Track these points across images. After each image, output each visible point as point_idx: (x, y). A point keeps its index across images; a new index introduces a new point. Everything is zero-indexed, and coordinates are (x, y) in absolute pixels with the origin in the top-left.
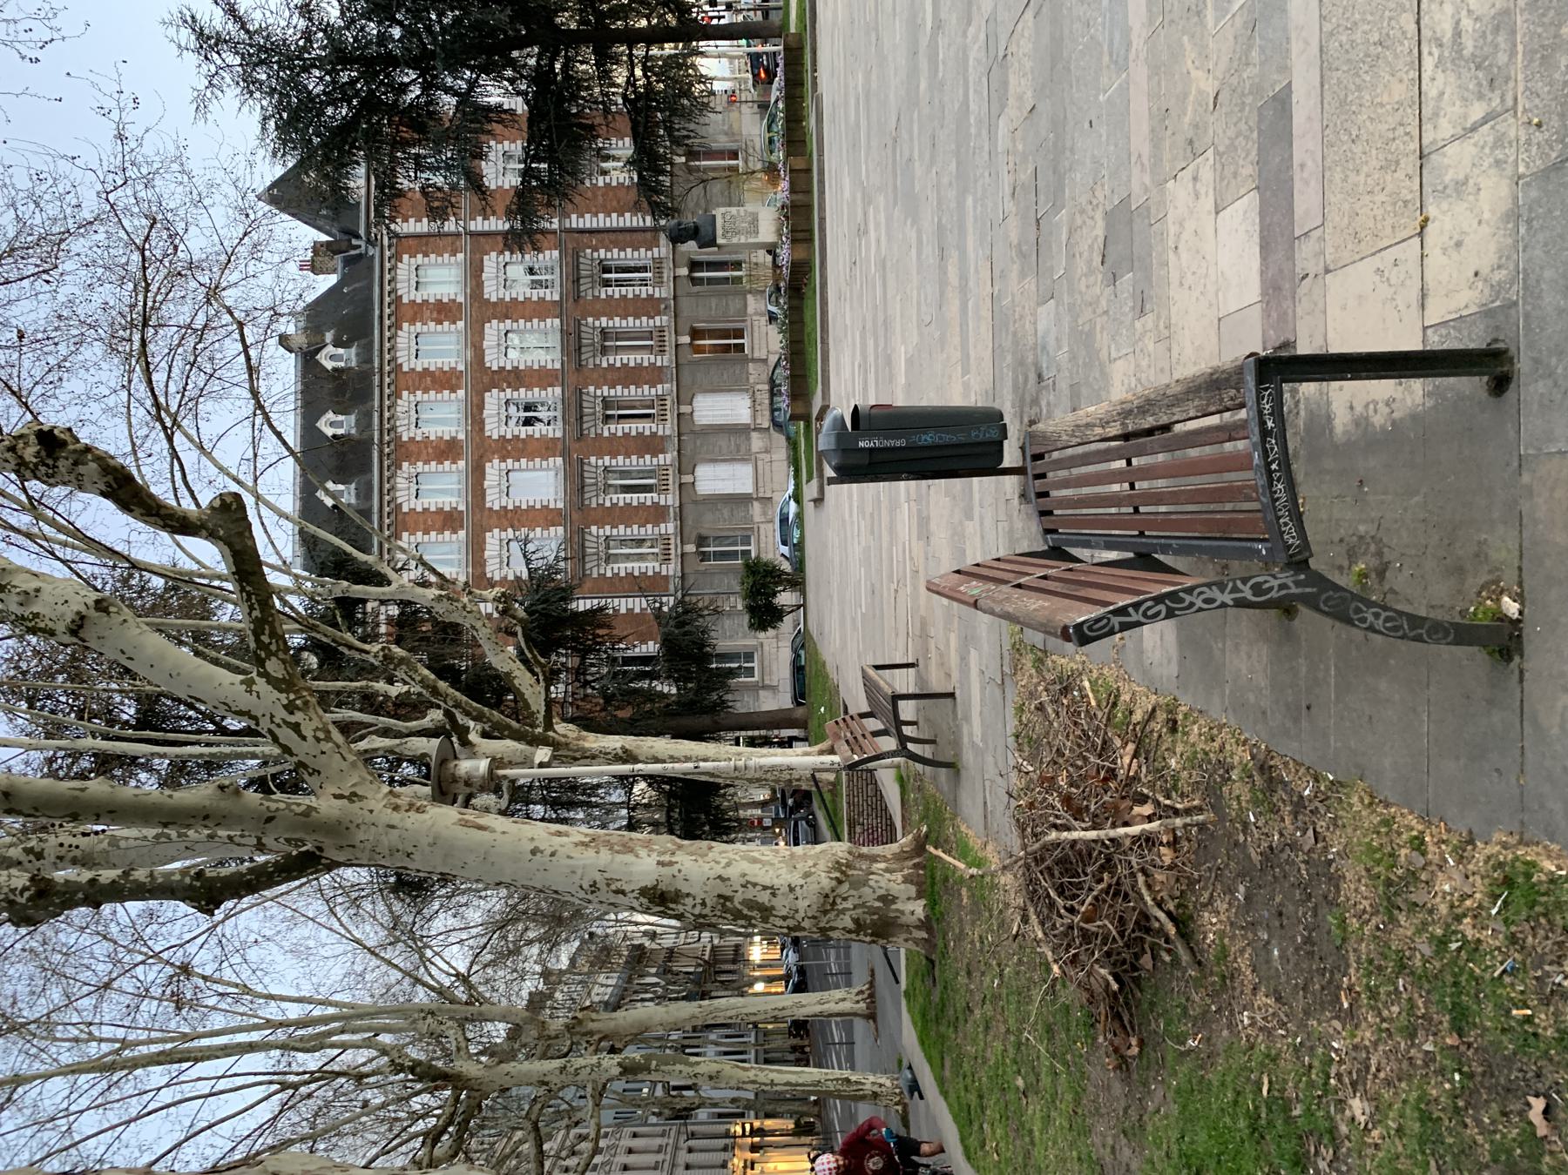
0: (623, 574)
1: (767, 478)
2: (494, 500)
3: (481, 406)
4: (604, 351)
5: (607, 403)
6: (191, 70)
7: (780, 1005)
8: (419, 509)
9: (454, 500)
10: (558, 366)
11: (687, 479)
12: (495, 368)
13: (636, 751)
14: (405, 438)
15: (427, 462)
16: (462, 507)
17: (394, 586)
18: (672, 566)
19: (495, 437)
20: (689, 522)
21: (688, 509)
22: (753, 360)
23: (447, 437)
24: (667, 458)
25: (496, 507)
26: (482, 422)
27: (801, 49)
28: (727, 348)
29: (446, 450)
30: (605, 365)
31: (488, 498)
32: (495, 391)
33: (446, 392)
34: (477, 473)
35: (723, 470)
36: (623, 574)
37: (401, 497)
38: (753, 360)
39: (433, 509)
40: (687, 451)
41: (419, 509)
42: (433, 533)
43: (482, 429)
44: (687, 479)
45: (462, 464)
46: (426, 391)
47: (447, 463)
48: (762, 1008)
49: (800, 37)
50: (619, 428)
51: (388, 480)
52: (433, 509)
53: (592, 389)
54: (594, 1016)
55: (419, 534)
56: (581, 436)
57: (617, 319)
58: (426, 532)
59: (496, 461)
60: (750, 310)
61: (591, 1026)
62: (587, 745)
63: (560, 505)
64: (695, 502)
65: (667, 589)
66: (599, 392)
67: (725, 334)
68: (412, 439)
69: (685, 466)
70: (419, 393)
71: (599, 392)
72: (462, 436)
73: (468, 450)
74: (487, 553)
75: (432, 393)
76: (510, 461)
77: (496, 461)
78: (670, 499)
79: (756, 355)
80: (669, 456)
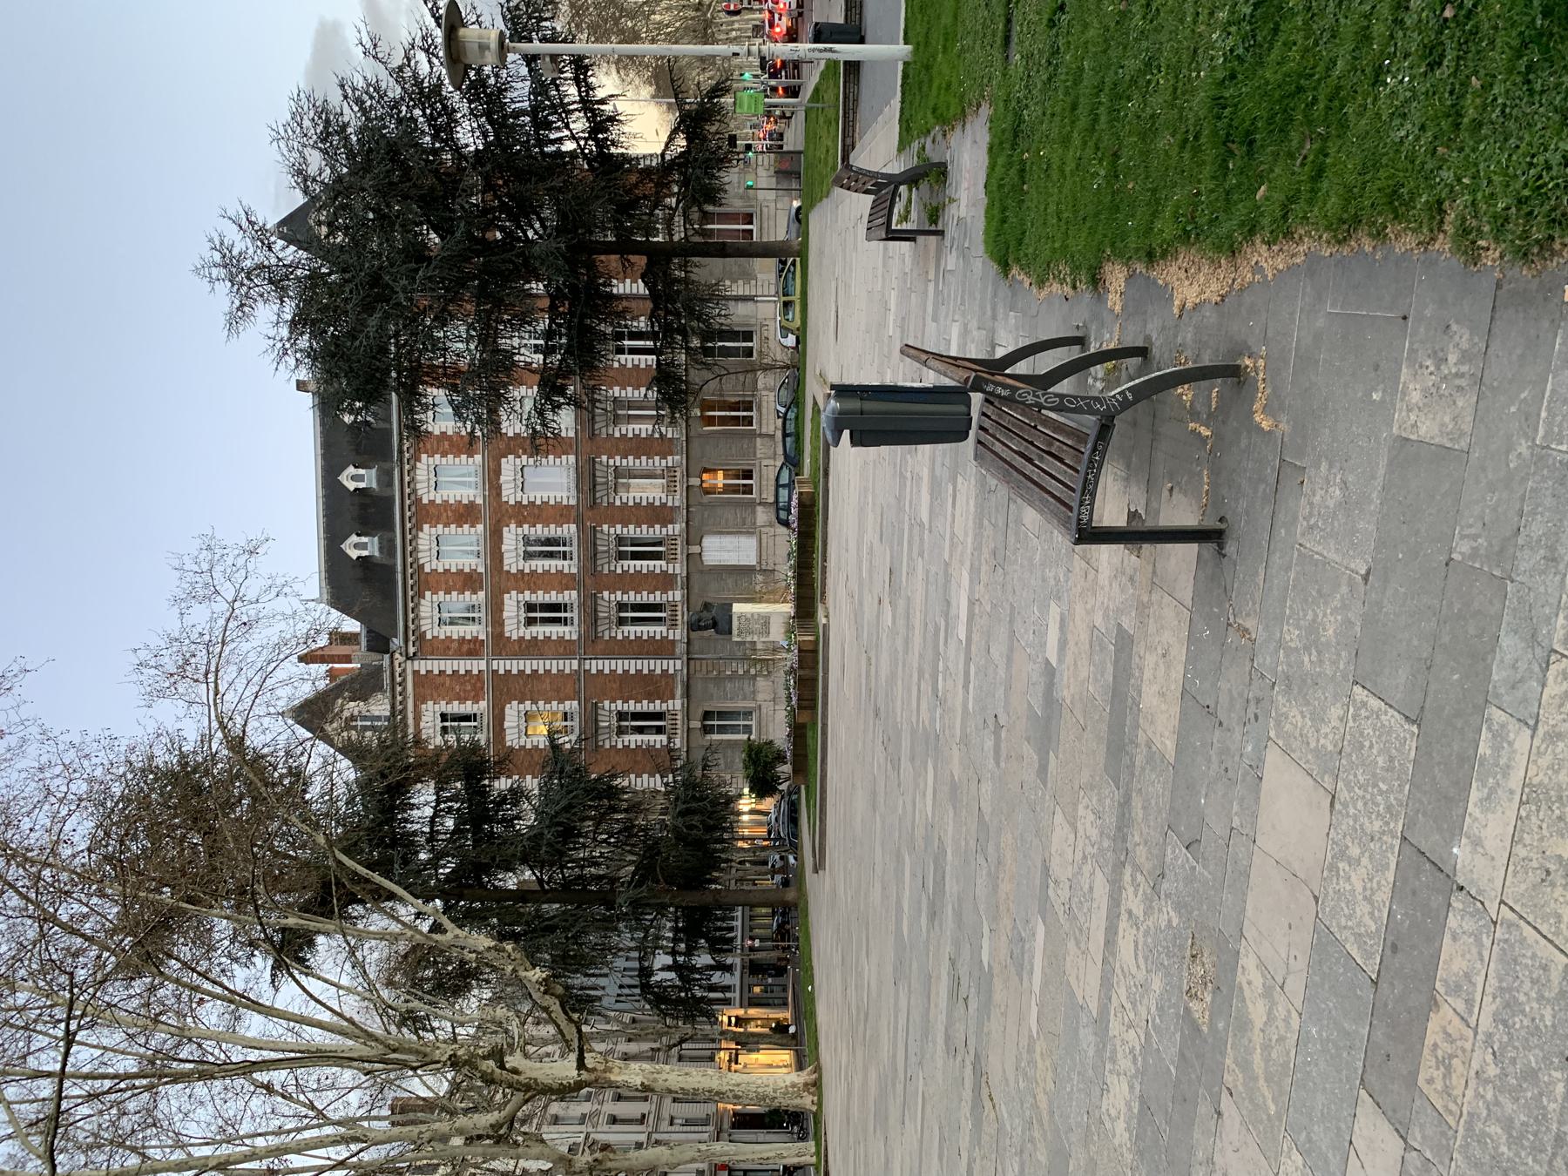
0: (632, 637)
1: (771, 551)
3: (498, 472)
4: (617, 420)
5: (621, 540)
6: (223, 297)
7: (765, 1155)
8: (441, 570)
9: (472, 492)
11: (695, 549)
12: (511, 434)
13: (654, 1085)
14: (425, 501)
15: (446, 525)
16: (481, 570)
17: (449, 936)
18: (678, 631)
19: (512, 502)
20: (695, 590)
21: (695, 578)
22: (761, 435)
23: (465, 501)
24: (676, 528)
25: (514, 571)
26: (499, 487)
27: (813, 504)
28: (736, 420)
29: (464, 514)
30: (617, 435)
31: (506, 562)
32: (511, 457)
33: (464, 457)
34: (495, 538)
35: (728, 541)
36: (632, 637)
37: (424, 557)
38: (761, 435)
39: (454, 570)
40: (694, 523)
41: (441, 570)
42: (454, 593)
43: (499, 495)
44: (695, 549)
45: (480, 527)
46: (444, 455)
47: (466, 526)
48: (750, 1157)
49: (813, 497)
51: (410, 543)
52: (454, 570)
53: (604, 458)
54: (611, 1156)
55: (441, 593)
56: (594, 504)
57: (630, 389)
58: (448, 592)
59: (513, 526)
60: (760, 385)
61: (609, 1165)
62: (613, 1078)
64: (702, 572)
65: (673, 652)
66: (611, 462)
67: (735, 407)
68: (432, 502)
69: (693, 537)
70: (437, 456)
71: (611, 462)
72: (479, 501)
73: (486, 513)
74: (505, 614)
75: (450, 457)
76: (526, 526)
77: (513, 526)
78: (678, 568)
79: (764, 431)
80: (677, 527)
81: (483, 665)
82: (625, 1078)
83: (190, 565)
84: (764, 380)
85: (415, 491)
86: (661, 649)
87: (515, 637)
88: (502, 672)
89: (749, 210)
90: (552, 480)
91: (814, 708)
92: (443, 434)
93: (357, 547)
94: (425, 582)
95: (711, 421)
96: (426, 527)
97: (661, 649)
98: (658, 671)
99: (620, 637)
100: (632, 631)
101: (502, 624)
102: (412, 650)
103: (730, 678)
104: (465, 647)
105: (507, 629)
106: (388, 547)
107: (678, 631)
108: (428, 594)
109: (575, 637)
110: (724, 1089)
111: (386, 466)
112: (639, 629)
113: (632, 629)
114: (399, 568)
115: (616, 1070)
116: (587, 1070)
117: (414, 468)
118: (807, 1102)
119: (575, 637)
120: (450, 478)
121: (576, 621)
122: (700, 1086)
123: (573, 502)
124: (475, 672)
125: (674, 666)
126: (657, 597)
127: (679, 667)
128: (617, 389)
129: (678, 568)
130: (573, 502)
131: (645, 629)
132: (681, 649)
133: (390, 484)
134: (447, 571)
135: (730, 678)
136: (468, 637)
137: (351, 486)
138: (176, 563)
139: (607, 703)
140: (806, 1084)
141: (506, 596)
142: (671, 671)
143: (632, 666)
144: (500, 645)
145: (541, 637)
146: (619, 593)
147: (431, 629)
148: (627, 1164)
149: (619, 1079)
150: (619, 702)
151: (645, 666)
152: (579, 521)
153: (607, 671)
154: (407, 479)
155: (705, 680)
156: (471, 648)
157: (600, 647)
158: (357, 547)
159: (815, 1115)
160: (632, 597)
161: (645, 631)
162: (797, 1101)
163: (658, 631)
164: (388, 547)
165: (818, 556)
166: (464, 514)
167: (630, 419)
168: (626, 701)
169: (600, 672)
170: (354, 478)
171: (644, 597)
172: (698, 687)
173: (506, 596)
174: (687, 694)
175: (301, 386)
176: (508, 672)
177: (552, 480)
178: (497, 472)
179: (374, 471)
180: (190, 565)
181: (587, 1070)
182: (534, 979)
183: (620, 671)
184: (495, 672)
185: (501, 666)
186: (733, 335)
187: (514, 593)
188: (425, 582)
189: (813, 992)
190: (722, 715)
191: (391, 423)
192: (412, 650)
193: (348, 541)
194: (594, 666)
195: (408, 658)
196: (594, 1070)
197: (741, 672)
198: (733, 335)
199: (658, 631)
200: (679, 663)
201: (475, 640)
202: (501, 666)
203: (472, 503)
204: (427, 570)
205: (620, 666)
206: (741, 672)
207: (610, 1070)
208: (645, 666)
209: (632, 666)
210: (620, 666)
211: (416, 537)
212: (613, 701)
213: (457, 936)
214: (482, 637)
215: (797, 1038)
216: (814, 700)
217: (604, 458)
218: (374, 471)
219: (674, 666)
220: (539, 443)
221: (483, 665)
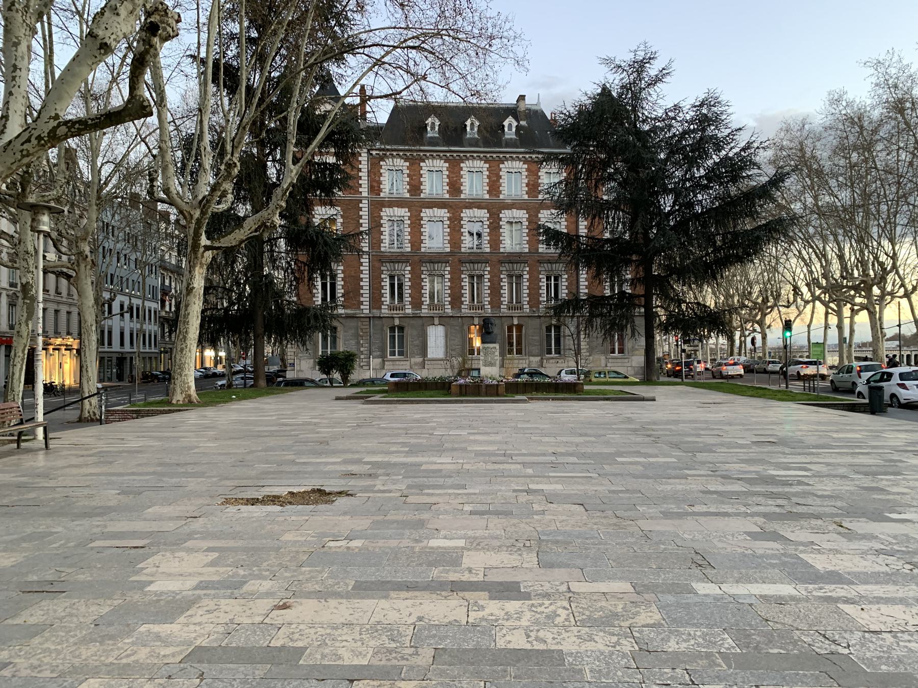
0: (383, 284)
1: (435, 366)
2: (426, 213)
3: (479, 207)
4: (510, 276)
7: (89, 369)
8: (422, 172)
10: (502, 250)
11: (436, 321)
12: (501, 215)
13: (192, 295)
14: (462, 165)
15: (448, 176)
16: (422, 196)
17: (292, 167)
18: (386, 311)
19: (462, 215)
20: (412, 322)
21: (420, 321)
23: (462, 188)
24: (448, 310)
25: (422, 215)
26: (471, 208)
27: (575, 392)
28: (511, 344)
29: (455, 187)
30: (502, 276)
31: (427, 210)
32: (488, 215)
33: (487, 188)
34: (441, 204)
35: (441, 341)
36: (383, 284)
37: (429, 162)
39: (422, 179)
40: (452, 321)
41: (422, 172)
42: (408, 179)
43: (466, 208)
44: (436, 321)
45: (447, 196)
46: (489, 177)
47: (447, 188)
48: (88, 360)
49: (582, 391)
50: (466, 283)
51: (437, 155)
52: (422, 179)
53: (489, 269)
54: (89, 267)
55: (408, 172)
56: (461, 262)
57: (528, 284)
58: (409, 176)
59: (448, 215)
60: (532, 358)
61: (82, 266)
62: (197, 269)
63: (423, 250)
64: (423, 325)
65: (374, 308)
66: (486, 273)
67: (519, 343)
68: (461, 169)
69: (444, 320)
70: (487, 173)
71: (486, 273)
72: (463, 196)
73: (455, 200)
74: (396, 209)
75: (487, 181)
76: (448, 222)
77: (448, 215)
78: (425, 311)
80: (450, 311)
81: (365, 194)
82: (197, 277)
83: (508, 26)
84: (535, 360)
85: (468, 159)
86: (376, 301)
87: (382, 214)
88: (361, 205)
89: (626, 352)
90: (513, 240)
91: (461, 395)
92: (500, 177)
93: (433, 123)
94: (415, 162)
95: (510, 329)
96: (447, 165)
97: (376, 301)
98: (362, 299)
99: (383, 276)
100: (386, 284)
101: (389, 207)
102: (374, 153)
103: (358, 343)
104: (375, 184)
105: (387, 209)
106: (433, 142)
107: (386, 311)
108: (408, 164)
109: (382, 249)
110: (188, 342)
111: (481, 143)
112: (388, 287)
113: (388, 284)
114: (422, 148)
115: (201, 271)
116: (204, 252)
117: (481, 159)
118: (178, 397)
119: (382, 249)
120: (514, 180)
121: (392, 250)
122: (190, 326)
123: (463, 250)
124: (360, 190)
125: (365, 308)
126: (407, 299)
127: (365, 311)
128: (527, 276)
129: (425, 311)
130: (463, 250)
131: (388, 291)
132: (376, 312)
133: (471, 145)
134: (421, 176)
135: (358, 343)
136: (382, 186)
137: (506, 123)
138: (510, 18)
139: (409, 268)
140: (190, 396)
141: (407, 210)
142: (362, 307)
143: (365, 283)
144: (377, 206)
145: (382, 229)
146: (409, 276)
147: (385, 165)
148: (83, 277)
149: (197, 273)
150: (342, 275)
151: (365, 291)
152: (451, 254)
153: (362, 268)
154: (475, 155)
155: (357, 328)
156: (375, 187)
157: (377, 264)
158: (433, 123)
159: (169, 403)
160: (407, 284)
161: (387, 291)
162: (179, 391)
163: (387, 299)
164: (433, 142)
165: (545, 395)
166: (455, 187)
167: (511, 284)
168: (343, 279)
169: (361, 264)
170: (510, 125)
171: (407, 291)
172: (352, 323)
173: (407, 210)
174: (415, 317)
175: (522, 98)
176: (361, 209)
177: (513, 240)
178: (480, 207)
179: (514, 137)
180: (508, 26)
181: (204, 252)
182: (275, 219)
183: (362, 276)
184: (361, 202)
185: (364, 205)
186: (621, 343)
187: (527, 216)
188: (415, 162)
189: (232, 400)
190: (401, 338)
191: (506, 147)
192: (374, 153)
193: (513, 120)
194: (365, 260)
195: (369, 150)
196: (203, 256)
197: (362, 349)
198: (621, 343)
199: (387, 299)
200: (368, 311)
201: (380, 190)
202: (364, 205)
203: (461, 192)
204: (422, 164)
205: (365, 276)
206: (362, 349)
207: (201, 267)
208: (365, 291)
209: (365, 283)
210: (365, 276)
211: (441, 158)
212: (343, 272)
213: (292, 171)
214: (382, 195)
215: (213, 387)
216: (466, 395)
217: (489, 269)
218: (514, 137)
219: (365, 308)
220: (535, 228)
221: (365, 194)
